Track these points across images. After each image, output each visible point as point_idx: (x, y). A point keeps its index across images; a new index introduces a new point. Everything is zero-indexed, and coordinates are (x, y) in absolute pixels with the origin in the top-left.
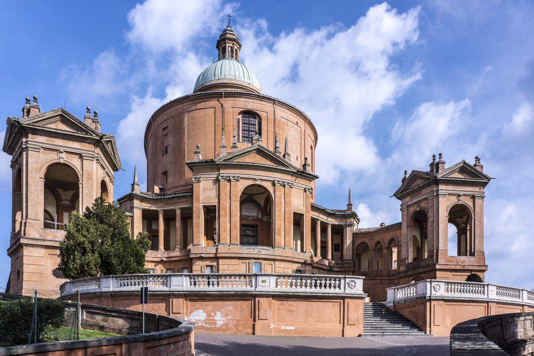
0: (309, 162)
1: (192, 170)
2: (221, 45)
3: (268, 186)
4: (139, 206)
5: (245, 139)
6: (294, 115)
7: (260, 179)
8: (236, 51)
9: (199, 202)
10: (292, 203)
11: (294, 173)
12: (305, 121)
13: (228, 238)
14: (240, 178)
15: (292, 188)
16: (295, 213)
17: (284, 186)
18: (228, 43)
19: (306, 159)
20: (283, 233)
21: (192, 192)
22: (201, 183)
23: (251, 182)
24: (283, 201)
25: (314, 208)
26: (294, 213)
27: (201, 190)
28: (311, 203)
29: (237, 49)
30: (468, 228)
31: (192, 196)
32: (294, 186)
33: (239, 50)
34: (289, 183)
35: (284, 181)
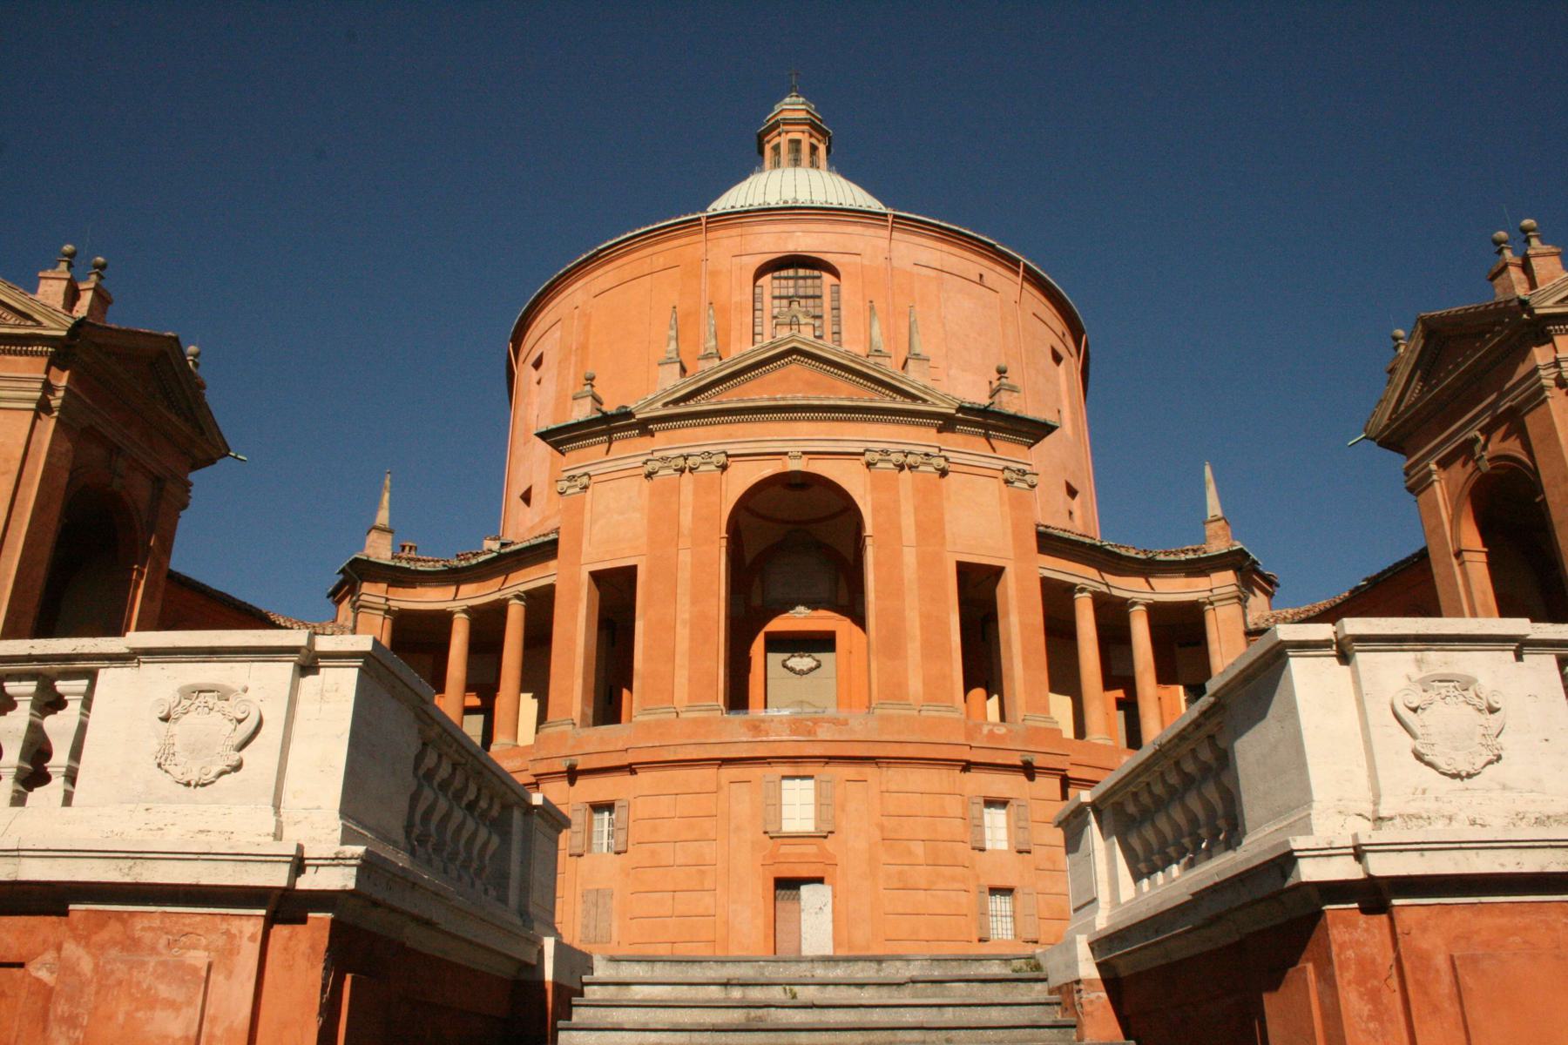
0: (1013, 378)
1: (563, 454)
2: (768, 142)
6: (967, 254)
7: (804, 453)
8: (814, 149)
10: (947, 526)
12: (1017, 273)
14: (728, 456)
15: (944, 473)
17: (911, 467)
18: (787, 132)
19: (1001, 372)
20: (914, 649)
21: (558, 533)
23: (768, 469)
25: (1049, 543)
27: (587, 516)
28: (1038, 525)
29: (814, 141)
31: (555, 542)
32: (952, 467)
33: (822, 148)
34: (927, 454)
35: (907, 448)
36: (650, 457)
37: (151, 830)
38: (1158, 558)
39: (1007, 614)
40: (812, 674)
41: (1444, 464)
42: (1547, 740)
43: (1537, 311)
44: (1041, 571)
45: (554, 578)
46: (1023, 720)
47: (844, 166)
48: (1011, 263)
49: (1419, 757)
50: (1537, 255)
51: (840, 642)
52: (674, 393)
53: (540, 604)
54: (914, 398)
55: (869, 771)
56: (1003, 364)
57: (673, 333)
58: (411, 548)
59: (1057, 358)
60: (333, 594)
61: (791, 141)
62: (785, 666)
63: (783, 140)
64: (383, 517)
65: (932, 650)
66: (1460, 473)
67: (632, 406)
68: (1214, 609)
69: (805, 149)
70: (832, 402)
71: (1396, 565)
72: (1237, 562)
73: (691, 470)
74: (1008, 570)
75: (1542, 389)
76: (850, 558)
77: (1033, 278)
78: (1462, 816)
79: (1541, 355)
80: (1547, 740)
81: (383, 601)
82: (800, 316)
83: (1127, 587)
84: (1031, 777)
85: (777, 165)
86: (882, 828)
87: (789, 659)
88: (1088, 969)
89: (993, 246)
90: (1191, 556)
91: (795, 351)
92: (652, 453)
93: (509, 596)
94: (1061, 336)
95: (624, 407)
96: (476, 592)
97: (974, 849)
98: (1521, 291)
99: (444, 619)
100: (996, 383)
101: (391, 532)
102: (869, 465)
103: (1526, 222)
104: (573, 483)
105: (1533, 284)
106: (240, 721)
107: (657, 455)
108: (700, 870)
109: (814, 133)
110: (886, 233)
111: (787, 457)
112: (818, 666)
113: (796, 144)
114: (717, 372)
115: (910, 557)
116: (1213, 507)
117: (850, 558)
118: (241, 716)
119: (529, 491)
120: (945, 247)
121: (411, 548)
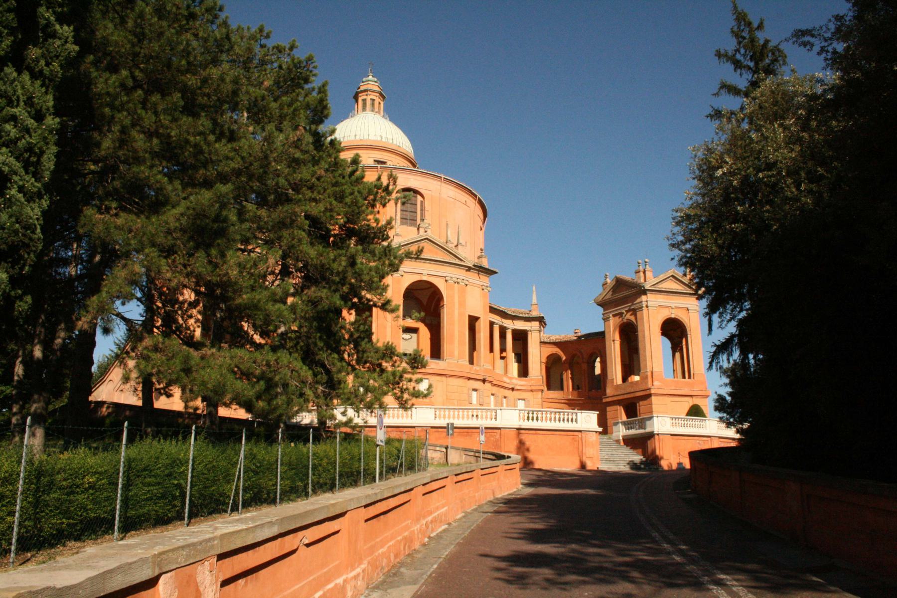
3: (440, 284)
5: (404, 221)
8: (379, 103)
25: (493, 310)
26: (470, 316)
30: (684, 343)
35: (458, 277)
39: (480, 332)
41: (614, 316)
47: (394, 115)
51: (420, 330)
54: (461, 260)
55: (444, 378)
61: (371, 99)
63: (368, 98)
66: (618, 320)
72: (541, 320)
74: (482, 319)
75: (642, 307)
77: (481, 203)
79: (644, 298)
83: (508, 323)
84: (484, 383)
88: (621, 438)
90: (527, 316)
98: (642, 280)
102: (446, 281)
103: (647, 260)
105: (645, 281)
110: (439, 183)
113: (373, 100)
115: (456, 312)
116: (534, 301)
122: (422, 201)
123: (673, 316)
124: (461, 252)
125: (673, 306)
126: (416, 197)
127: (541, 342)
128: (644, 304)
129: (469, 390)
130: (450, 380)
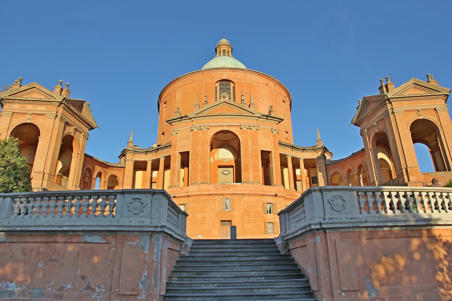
1: (172, 126)
4: (131, 159)
6: (264, 79)
9: (176, 150)
10: (259, 142)
11: (260, 118)
13: (199, 178)
16: (262, 152)
20: (251, 170)
22: (178, 135)
24: (250, 142)
26: (261, 150)
27: (178, 140)
29: (229, 50)
33: (230, 51)
34: (254, 126)
35: (250, 125)
36: (192, 126)
37: (129, 222)
38: (306, 149)
40: (228, 175)
42: (354, 205)
43: (388, 97)
44: (280, 152)
45: (171, 154)
46: (275, 185)
48: (273, 80)
49: (332, 208)
50: (390, 84)
52: (197, 112)
53: (168, 159)
56: (272, 105)
57: (197, 98)
58: (137, 146)
59: (284, 102)
60: (119, 157)
62: (222, 173)
64: (131, 139)
65: (255, 169)
67: (188, 115)
68: (318, 160)
69: (227, 52)
70: (233, 114)
71: (358, 152)
73: (201, 129)
74: (273, 152)
75: (389, 114)
76: (237, 148)
78: (339, 218)
80: (354, 205)
81: (131, 159)
82: (226, 94)
85: (220, 56)
86: (244, 209)
87: (223, 171)
89: (269, 77)
91: (225, 102)
92: (192, 126)
93: (160, 158)
94: (285, 97)
95: (186, 115)
96: (153, 156)
97: (264, 214)
99: (146, 162)
100: (270, 110)
101: (133, 143)
102: (241, 128)
104: (174, 132)
105: (388, 91)
106: (143, 204)
107: (194, 126)
108: (204, 219)
109: (228, 47)
111: (223, 126)
112: (230, 173)
114: (207, 107)
116: (319, 137)
117: (237, 148)
118: (143, 203)
119: (164, 133)
120: (258, 77)
121: (137, 146)
122: (234, 87)
123: (421, 118)
124: (251, 109)
125: (419, 108)
126: (230, 84)
127: (326, 166)
128: (390, 112)
129: (263, 203)
130: (246, 198)
